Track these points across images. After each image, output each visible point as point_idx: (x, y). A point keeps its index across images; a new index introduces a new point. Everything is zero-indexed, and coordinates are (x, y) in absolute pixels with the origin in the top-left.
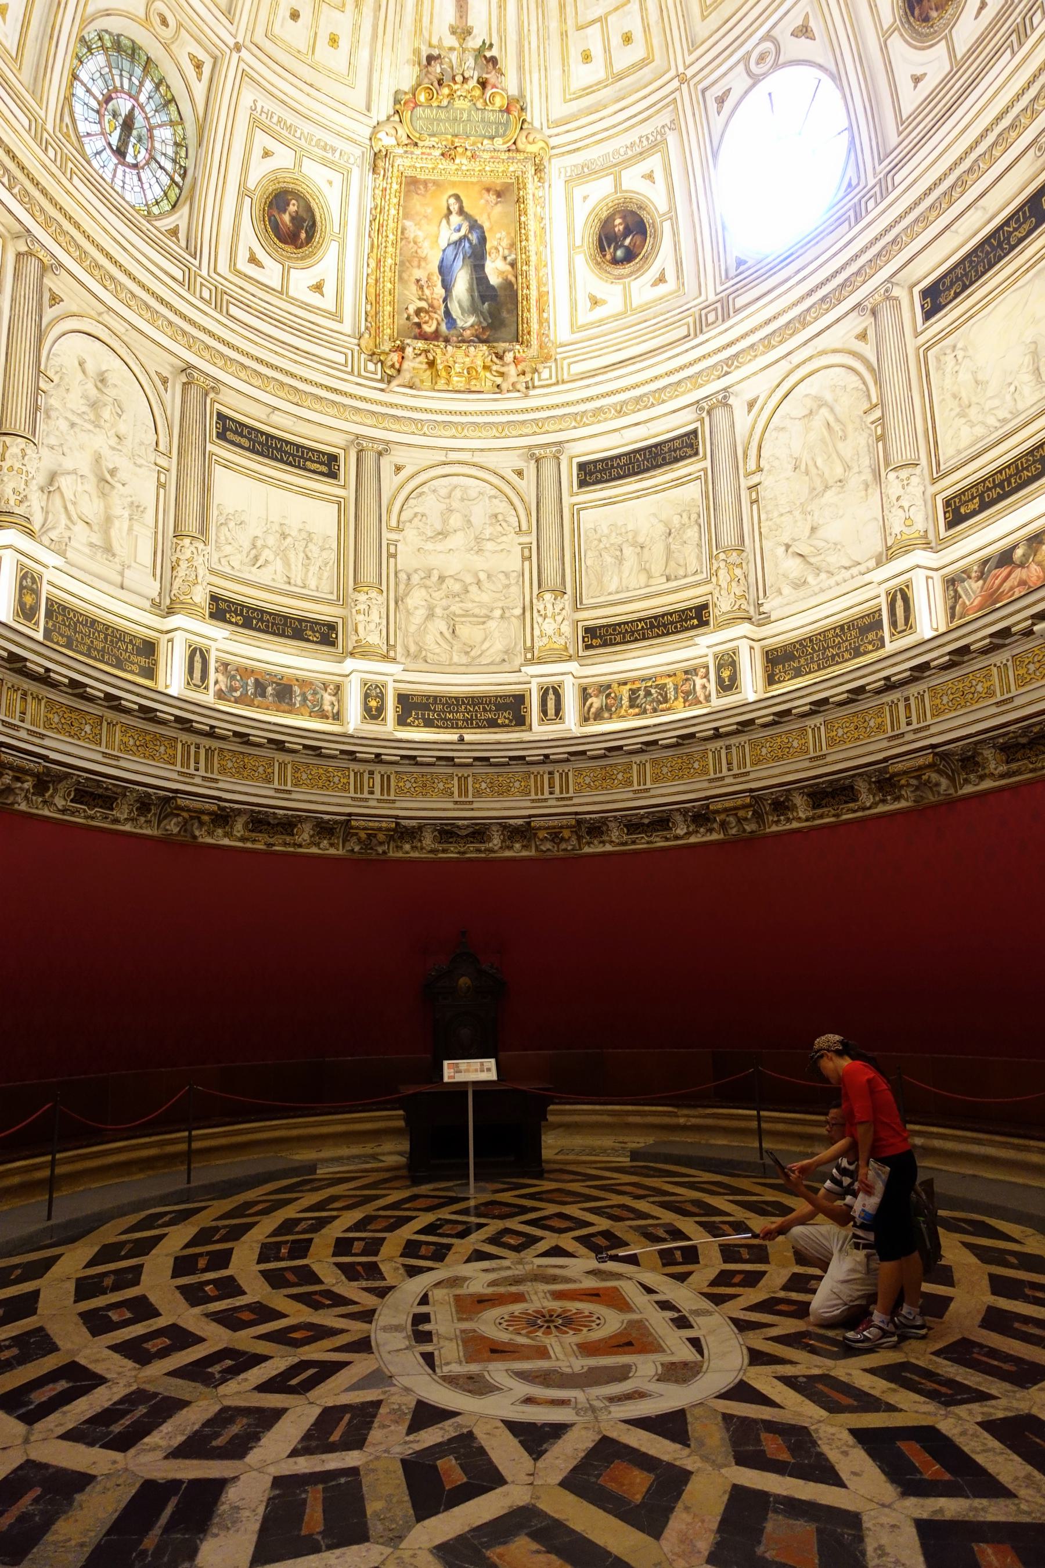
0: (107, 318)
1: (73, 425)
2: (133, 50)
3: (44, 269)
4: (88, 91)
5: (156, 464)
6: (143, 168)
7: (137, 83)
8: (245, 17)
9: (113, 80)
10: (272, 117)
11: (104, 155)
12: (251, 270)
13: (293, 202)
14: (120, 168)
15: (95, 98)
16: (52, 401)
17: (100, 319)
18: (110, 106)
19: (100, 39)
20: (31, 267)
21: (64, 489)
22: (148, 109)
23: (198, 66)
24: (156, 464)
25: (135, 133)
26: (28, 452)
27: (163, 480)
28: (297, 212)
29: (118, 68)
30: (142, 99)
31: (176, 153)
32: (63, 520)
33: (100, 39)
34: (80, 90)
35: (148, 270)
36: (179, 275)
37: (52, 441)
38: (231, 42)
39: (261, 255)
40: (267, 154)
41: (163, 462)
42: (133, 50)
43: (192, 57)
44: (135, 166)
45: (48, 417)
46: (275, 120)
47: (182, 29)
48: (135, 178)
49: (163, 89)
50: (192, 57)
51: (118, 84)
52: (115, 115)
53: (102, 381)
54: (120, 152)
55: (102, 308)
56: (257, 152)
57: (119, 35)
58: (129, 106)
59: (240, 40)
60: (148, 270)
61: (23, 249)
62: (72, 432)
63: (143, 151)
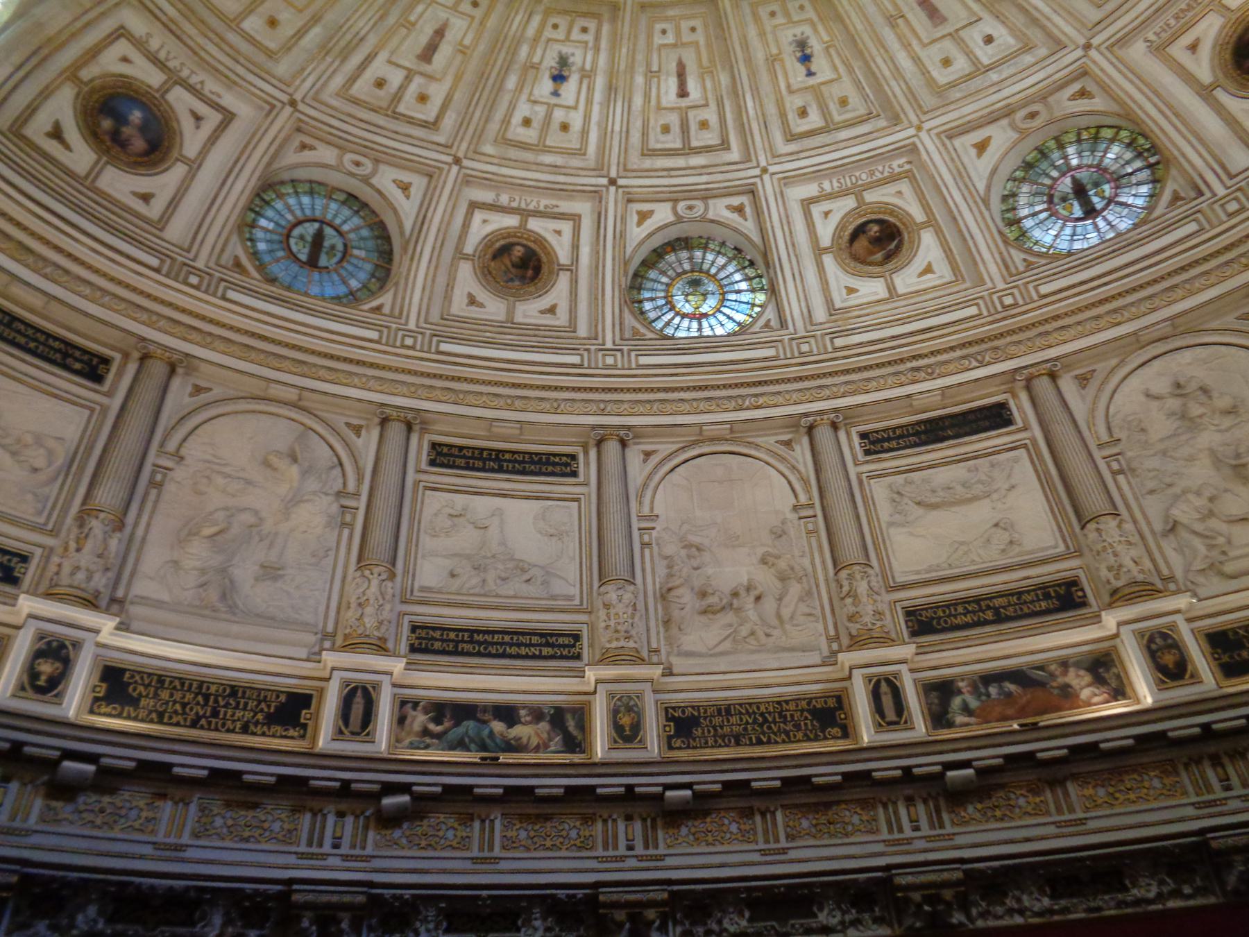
1: (1164, 453)
3: (1053, 376)
4: (1034, 215)
6: (1116, 195)
9: (1044, 185)
10: (1168, 25)
11: (1079, 230)
14: (1101, 223)
15: (1041, 212)
16: (1130, 454)
18: (1056, 200)
19: (1015, 180)
20: (1043, 385)
21: (1183, 519)
22: (1085, 161)
23: (1083, 94)
25: (1089, 187)
26: (1101, 527)
30: (1074, 162)
32: (1198, 543)
33: (1015, 180)
34: (1028, 223)
36: (1193, 227)
37: (1151, 485)
38: (1079, 53)
43: (1071, 99)
44: (1110, 201)
45: (1133, 470)
46: (1172, 22)
48: (1118, 209)
49: (1085, 135)
50: (1073, 98)
51: (1047, 182)
53: (1178, 386)
54: (1090, 212)
55: (1133, 338)
56: (1185, 58)
57: (1024, 161)
58: (1068, 181)
59: (1082, 41)
61: (1024, 383)
63: (1106, 187)
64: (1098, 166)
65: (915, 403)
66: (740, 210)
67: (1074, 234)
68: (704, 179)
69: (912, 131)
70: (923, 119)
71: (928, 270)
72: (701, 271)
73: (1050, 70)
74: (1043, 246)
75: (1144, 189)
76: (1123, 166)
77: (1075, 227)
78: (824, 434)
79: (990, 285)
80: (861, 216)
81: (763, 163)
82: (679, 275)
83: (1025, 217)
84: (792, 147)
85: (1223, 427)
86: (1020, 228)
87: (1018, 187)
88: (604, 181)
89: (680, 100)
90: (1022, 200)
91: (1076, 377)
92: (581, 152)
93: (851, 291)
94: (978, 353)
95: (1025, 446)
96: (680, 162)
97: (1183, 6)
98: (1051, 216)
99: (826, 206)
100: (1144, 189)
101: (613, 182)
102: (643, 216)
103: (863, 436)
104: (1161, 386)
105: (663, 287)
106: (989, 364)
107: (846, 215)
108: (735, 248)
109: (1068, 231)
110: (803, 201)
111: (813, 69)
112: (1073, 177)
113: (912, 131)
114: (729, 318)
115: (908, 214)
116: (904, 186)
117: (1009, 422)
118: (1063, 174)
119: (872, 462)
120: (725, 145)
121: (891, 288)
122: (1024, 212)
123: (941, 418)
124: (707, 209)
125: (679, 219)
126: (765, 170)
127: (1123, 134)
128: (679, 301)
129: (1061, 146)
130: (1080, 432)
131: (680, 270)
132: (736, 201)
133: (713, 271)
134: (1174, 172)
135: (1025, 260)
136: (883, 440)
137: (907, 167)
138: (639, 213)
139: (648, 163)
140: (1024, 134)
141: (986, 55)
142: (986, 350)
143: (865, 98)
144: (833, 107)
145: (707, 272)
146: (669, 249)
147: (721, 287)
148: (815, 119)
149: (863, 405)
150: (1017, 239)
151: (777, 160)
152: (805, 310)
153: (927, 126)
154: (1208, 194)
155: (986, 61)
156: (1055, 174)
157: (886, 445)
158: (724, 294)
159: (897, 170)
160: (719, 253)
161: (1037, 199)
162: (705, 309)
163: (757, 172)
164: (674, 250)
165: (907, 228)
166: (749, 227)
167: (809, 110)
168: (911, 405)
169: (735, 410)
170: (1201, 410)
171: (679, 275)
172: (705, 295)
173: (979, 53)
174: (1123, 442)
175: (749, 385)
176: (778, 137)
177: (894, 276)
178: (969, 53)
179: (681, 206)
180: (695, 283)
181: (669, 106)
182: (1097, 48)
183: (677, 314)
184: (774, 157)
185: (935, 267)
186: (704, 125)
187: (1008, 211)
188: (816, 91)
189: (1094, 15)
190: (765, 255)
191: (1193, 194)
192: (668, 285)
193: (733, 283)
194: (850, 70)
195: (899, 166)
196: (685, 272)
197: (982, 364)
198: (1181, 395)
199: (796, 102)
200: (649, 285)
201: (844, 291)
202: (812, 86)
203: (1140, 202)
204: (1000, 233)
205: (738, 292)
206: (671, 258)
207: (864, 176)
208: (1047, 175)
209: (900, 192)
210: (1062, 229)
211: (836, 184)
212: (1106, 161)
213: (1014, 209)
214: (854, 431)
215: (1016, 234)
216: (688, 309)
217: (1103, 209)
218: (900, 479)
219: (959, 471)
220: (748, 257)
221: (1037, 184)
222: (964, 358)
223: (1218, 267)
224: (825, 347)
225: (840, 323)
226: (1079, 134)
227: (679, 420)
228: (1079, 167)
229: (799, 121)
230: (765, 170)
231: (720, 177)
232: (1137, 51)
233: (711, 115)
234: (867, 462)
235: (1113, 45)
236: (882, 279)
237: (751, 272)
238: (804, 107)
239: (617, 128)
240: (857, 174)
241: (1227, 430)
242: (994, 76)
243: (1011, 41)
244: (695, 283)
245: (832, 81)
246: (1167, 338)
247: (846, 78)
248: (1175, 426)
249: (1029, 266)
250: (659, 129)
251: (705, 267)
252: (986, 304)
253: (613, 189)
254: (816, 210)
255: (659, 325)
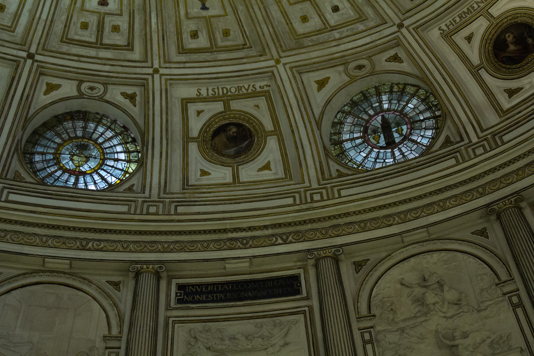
0: (408, 239)
2: (364, 95)
4: (353, 139)
5: (504, 294)
6: (411, 134)
7: (377, 104)
8: (389, 11)
9: (363, 119)
10: (455, 21)
11: (381, 155)
12: (517, 99)
13: (507, 35)
15: (358, 138)
16: (378, 328)
17: (406, 244)
18: (369, 131)
19: (343, 112)
22: (393, 107)
23: (396, 58)
24: (504, 294)
25: (393, 125)
27: (515, 300)
28: (514, 37)
29: (361, 111)
30: (386, 106)
31: (427, 104)
33: (343, 112)
34: (347, 145)
35: (412, 187)
38: (395, 29)
39: (513, 84)
40: (469, 39)
41: (507, 288)
42: (364, 95)
43: (389, 60)
44: (406, 138)
45: (377, 341)
46: (458, 19)
47: (373, 58)
48: (410, 144)
49: (395, 89)
50: (389, 60)
51: (366, 117)
52: (375, 131)
53: (425, 280)
54: (391, 144)
55: (399, 238)
57: (351, 100)
58: (379, 118)
59: (397, 21)
60: (412, 187)
62: (405, 335)
63: (405, 127)
64: (401, 112)
65: (227, 266)
66: (132, 98)
67: (377, 158)
68: (107, 68)
69: (272, 63)
70: (282, 54)
71: (267, 167)
72: (90, 139)
73: (374, 37)
74: (355, 163)
75: (429, 133)
76: (418, 114)
77: (379, 152)
78: (147, 281)
79: (307, 184)
80: (226, 119)
81: (156, 66)
82: (71, 139)
83: (346, 141)
84: (183, 58)
85: (449, 315)
86: (341, 148)
87: (345, 118)
88: (24, 54)
89: (100, 7)
90: (346, 128)
91: (354, 263)
92: (11, 29)
93: (204, 173)
94: (284, 234)
95: (304, 312)
96: (92, 52)
97: (465, 10)
98: (363, 142)
99: (200, 106)
100: (429, 133)
101: (31, 56)
102: (51, 88)
103: (180, 287)
104: (412, 278)
105: (55, 146)
106: (291, 242)
107: (215, 115)
108: (124, 127)
109: (373, 155)
110: (183, 100)
111: (207, 5)
112: (383, 117)
113: (272, 63)
114: (103, 178)
115: (261, 124)
116: (262, 102)
117: (298, 292)
118: (377, 114)
119: (181, 309)
120: (130, 46)
121: (236, 176)
122: (346, 137)
123: (246, 282)
124: (105, 92)
125: (81, 95)
126: (156, 71)
127: (421, 92)
128: (64, 159)
129: (379, 94)
130: (346, 305)
131: (72, 135)
132: (130, 90)
133: (100, 140)
134: (449, 122)
135: (338, 170)
136: (197, 293)
137: (266, 89)
138: (48, 84)
139: (65, 48)
140: (353, 80)
141: (333, 19)
142: (290, 233)
143: (243, 32)
144: (219, 36)
145: (96, 141)
146: (69, 117)
147: (104, 154)
148: (203, 41)
149: (185, 261)
150: (338, 155)
151: (167, 65)
152: (163, 182)
153: (283, 61)
154: (466, 141)
155: (332, 23)
156: (371, 112)
157: (197, 297)
158: (104, 159)
159: (258, 89)
160: (109, 128)
161: (356, 129)
162: (85, 168)
163: (150, 71)
164: (72, 119)
165: (258, 134)
166: (136, 111)
167: (200, 34)
168: (225, 268)
169: (78, 249)
170: (433, 301)
171: (71, 139)
172: (87, 159)
173: (328, 16)
174: (377, 318)
175: (95, 231)
176: (173, 49)
177: (240, 167)
178: (321, 15)
179: (84, 87)
180: (83, 148)
181: (91, 9)
182: (407, 28)
183: (60, 168)
184: (165, 62)
185: (272, 166)
186: (116, 29)
187: (335, 134)
188: (208, 20)
189: (409, 5)
190: (143, 135)
191: (458, 139)
192: (59, 145)
193: (114, 153)
194: (235, 11)
195: (260, 87)
196: (77, 137)
197: (285, 242)
198: (425, 287)
199: (189, 26)
200: (44, 142)
201: (199, 173)
202: (204, 17)
203: (425, 141)
204: (324, 148)
205: (117, 160)
206: (69, 125)
207: (233, 90)
208: (366, 113)
209: (257, 106)
210: (370, 153)
211: (210, 92)
212: (408, 109)
213: (340, 133)
214: (174, 282)
215: (338, 152)
216: (71, 166)
217: (400, 143)
218: (199, 326)
219: (248, 326)
220: (132, 135)
221: (358, 117)
222: (273, 235)
223: (462, 194)
224: (169, 210)
225: (187, 195)
226: (392, 87)
227: (26, 249)
228: (389, 110)
229: (190, 40)
230: (156, 71)
231: (120, 69)
232: (434, 34)
233: (123, 23)
234: (177, 309)
235: (418, 27)
236: (231, 169)
237: (131, 147)
238: (196, 31)
239: (44, 17)
240: (229, 88)
241: (451, 317)
242: (336, 34)
243: (352, 13)
244: (83, 148)
245: (220, 16)
246: (423, 242)
247: (231, 17)
248: (417, 310)
249: (340, 175)
250: (79, 25)
251: (95, 136)
252: (300, 198)
253: (29, 62)
254: (192, 108)
255: (43, 174)
